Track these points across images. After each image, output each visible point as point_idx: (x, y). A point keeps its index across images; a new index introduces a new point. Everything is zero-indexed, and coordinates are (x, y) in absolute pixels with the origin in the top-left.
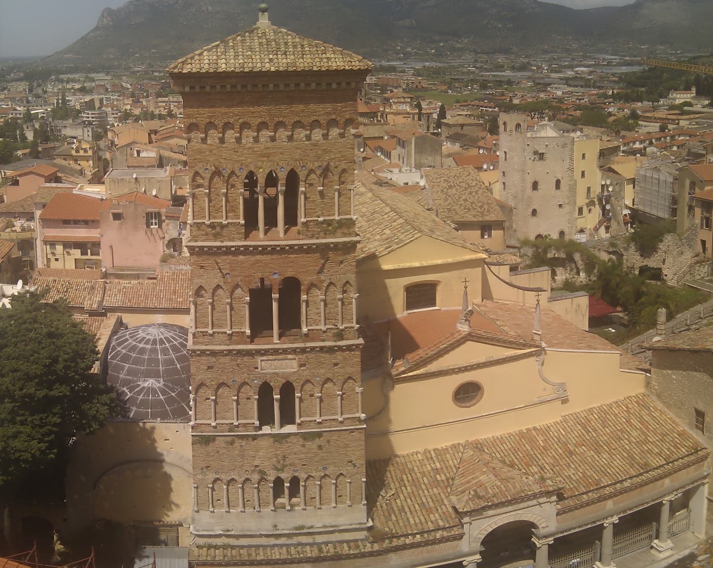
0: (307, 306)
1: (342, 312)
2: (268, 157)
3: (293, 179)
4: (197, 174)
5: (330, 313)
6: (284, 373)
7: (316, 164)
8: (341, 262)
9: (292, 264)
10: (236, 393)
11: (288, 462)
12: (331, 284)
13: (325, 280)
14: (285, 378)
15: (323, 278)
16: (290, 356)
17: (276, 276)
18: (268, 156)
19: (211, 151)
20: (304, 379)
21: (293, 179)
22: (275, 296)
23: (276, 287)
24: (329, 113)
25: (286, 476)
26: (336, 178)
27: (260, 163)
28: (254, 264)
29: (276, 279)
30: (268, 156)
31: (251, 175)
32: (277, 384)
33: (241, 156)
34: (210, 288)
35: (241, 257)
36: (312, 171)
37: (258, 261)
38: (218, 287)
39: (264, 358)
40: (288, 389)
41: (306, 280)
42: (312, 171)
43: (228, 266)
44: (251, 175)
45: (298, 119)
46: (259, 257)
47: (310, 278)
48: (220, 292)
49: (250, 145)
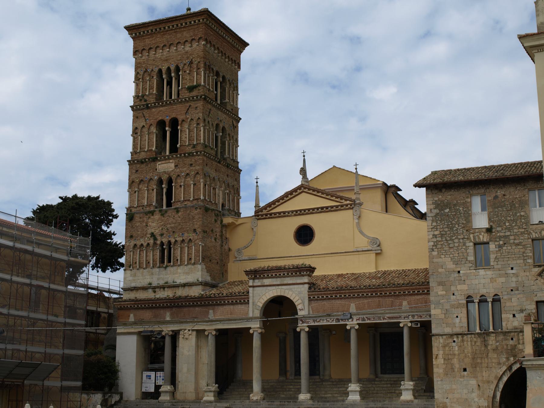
0: (181, 132)
1: (197, 136)
2: (167, 61)
3: (178, 69)
4: (138, 73)
5: (191, 136)
6: (168, 171)
7: (187, 61)
9: (175, 111)
10: (146, 186)
12: (192, 119)
13: (189, 118)
14: (168, 174)
15: (188, 116)
16: (171, 161)
17: (168, 118)
18: (167, 60)
19: (144, 62)
21: (178, 69)
22: (167, 128)
24: (192, 36)
25: (165, 240)
27: (163, 64)
28: (159, 112)
29: (167, 119)
30: (167, 60)
31: (160, 71)
32: (165, 178)
33: (156, 62)
34: (139, 128)
35: (154, 110)
36: (185, 64)
38: (144, 126)
39: (160, 163)
40: (170, 182)
41: (180, 118)
43: (148, 115)
44: (160, 71)
45: (179, 41)
46: (161, 108)
47: (182, 117)
49: (159, 57)
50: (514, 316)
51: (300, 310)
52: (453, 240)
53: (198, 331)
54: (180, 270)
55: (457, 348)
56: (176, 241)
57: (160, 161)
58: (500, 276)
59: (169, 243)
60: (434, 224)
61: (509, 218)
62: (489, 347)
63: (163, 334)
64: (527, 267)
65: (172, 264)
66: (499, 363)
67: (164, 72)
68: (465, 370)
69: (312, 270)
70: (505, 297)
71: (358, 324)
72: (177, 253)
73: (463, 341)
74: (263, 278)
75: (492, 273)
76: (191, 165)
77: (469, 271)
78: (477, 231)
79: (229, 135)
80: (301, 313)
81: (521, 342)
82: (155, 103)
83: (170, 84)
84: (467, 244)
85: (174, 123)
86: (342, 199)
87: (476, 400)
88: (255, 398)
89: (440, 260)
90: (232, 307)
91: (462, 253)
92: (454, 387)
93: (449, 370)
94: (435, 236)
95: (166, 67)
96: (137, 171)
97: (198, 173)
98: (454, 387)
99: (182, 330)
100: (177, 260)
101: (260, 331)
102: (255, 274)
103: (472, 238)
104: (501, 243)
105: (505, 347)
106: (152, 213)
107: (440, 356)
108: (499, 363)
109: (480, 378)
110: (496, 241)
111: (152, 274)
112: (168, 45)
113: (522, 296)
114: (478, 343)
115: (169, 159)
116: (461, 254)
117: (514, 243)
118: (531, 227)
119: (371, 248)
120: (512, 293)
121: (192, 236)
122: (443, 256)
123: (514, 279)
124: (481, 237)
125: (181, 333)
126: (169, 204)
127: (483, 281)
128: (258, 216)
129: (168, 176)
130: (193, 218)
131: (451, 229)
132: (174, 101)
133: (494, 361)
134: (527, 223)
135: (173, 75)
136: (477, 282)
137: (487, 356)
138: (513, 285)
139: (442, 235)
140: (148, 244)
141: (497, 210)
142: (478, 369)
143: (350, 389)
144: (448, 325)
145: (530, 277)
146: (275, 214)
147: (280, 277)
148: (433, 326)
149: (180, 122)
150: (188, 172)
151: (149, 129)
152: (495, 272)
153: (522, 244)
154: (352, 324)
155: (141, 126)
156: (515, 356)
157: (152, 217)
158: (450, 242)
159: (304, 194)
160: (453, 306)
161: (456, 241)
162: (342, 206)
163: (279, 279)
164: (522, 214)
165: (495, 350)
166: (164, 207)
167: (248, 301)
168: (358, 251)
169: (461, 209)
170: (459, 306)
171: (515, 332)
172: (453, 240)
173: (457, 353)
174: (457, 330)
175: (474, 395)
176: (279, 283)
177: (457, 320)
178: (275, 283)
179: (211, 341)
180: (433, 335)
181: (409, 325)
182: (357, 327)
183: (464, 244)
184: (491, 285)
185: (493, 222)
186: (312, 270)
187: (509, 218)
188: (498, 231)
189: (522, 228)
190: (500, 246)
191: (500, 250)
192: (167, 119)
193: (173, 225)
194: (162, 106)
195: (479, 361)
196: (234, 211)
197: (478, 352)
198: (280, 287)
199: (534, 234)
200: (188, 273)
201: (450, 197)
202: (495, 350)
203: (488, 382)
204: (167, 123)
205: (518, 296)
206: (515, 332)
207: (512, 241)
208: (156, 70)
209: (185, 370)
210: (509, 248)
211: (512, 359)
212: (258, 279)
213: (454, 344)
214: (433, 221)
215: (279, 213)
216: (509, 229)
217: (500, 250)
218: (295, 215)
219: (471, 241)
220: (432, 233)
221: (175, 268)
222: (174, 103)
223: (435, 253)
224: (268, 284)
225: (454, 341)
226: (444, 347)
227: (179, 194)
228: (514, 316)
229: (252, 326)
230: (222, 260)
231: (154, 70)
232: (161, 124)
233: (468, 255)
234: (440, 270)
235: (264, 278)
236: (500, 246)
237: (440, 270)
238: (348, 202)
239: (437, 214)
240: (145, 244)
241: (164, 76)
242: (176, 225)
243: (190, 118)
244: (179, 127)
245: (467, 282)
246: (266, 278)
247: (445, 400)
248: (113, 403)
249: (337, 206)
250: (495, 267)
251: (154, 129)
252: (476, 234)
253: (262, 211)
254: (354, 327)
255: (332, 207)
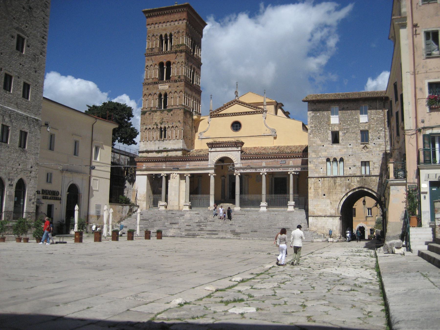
8: (181, 56)
11: (163, 121)
12: (179, 62)
16: (167, 84)
20: (170, 91)
21: (171, 35)
23: (165, 64)
26: (181, 34)
31: (161, 36)
32: (163, 93)
37: (161, 57)
38: (151, 65)
40: (166, 95)
41: (172, 62)
42: (175, 33)
44: (161, 36)
46: (162, 56)
48: (151, 66)
50: (350, 168)
51: (237, 164)
52: (320, 129)
53: (180, 174)
54: (171, 142)
55: (321, 184)
56: (169, 127)
57: (160, 84)
58: (344, 148)
59: (165, 128)
60: (312, 121)
61: (349, 119)
62: (337, 184)
63: (162, 175)
64: (357, 144)
65: (166, 139)
66: (342, 192)
67: (163, 36)
68: (324, 195)
69: (242, 144)
70: (346, 159)
71: (266, 172)
72: (169, 133)
73: (324, 181)
74: (216, 148)
75: (340, 146)
76: (178, 87)
77: (328, 146)
78: (333, 125)
79: (196, 72)
80: (236, 166)
81: (353, 181)
82: (158, 53)
83: (166, 43)
84: (328, 132)
85: (169, 64)
86: (257, 108)
87: (329, 210)
88: (211, 209)
89: (314, 139)
90: (199, 162)
91: (325, 136)
92: (319, 203)
93: (317, 194)
94: (312, 127)
95: (165, 34)
96: (148, 89)
97: (181, 91)
98: (319, 203)
99: (171, 173)
100: (169, 137)
101: (214, 175)
102: (212, 145)
103: (331, 129)
104: (345, 131)
105: (345, 184)
106: (156, 111)
107: (312, 188)
108: (342, 192)
109: (332, 199)
110: (342, 131)
111: (155, 144)
112: (166, 22)
113: (354, 158)
114: (332, 182)
115: (165, 83)
116: (325, 137)
117: (351, 132)
118: (360, 124)
119: (271, 134)
120: (350, 157)
121: (178, 124)
122: (315, 137)
123: (351, 150)
124: (335, 128)
125: (171, 175)
126: (165, 107)
127: (335, 151)
128: (212, 115)
129: (164, 92)
130: (179, 115)
131: (320, 123)
132: (169, 52)
133: (339, 190)
134: (358, 122)
135: (168, 38)
136: (332, 151)
137: (335, 189)
138: (350, 153)
139: (315, 127)
140: (153, 128)
141: (343, 115)
142: (331, 194)
143: (261, 205)
144: (317, 172)
145: (359, 149)
146: (221, 114)
147: (226, 147)
148: (309, 173)
149: (172, 64)
150: (176, 90)
151: (154, 66)
152: (341, 146)
153: (356, 132)
154: (264, 171)
155: (150, 65)
156: (349, 188)
157: (156, 114)
158: (319, 130)
159: (236, 104)
160: (319, 163)
161: (322, 130)
162: (257, 112)
163: (225, 148)
164: (356, 117)
165: (340, 185)
166: (163, 109)
167: (208, 159)
168: (265, 136)
169: (325, 114)
170: (322, 163)
171: (350, 177)
172: (320, 129)
173: (321, 186)
174: (321, 175)
175: (329, 207)
176: (225, 150)
177: (322, 170)
178: (222, 150)
179: (188, 179)
180: (309, 178)
181: (293, 173)
182: (266, 174)
183: (326, 132)
184: (339, 153)
185: (342, 121)
186: (242, 144)
187: (349, 119)
188: (344, 126)
189: (356, 125)
190: (345, 133)
191: (344, 135)
192: (165, 62)
193: (167, 118)
194: (162, 54)
195: (332, 190)
196: (197, 112)
197: (331, 186)
198: (225, 152)
199: (361, 128)
200: (175, 144)
201: (320, 107)
202: (340, 185)
203: (336, 201)
204: (165, 64)
205: (353, 159)
206: (350, 177)
207: (350, 131)
208: (159, 35)
209: (173, 194)
210: (349, 134)
211: (348, 190)
212: (214, 148)
213: (319, 182)
214: (311, 119)
215: (223, 114)
216: (350, 125)
217: (344, 135)
218: (231, 116)
219: (330, 130)
220: (310, 125)
221: (168, 141)
222: (170, 53)
223: (311, 136)
224: (219, 150)
225: (320, 181)
226: (314, 183)
227: (171, 102)
228: (350, 168)
229: (210, 172)
230: (192, 138)
231: (158, 35)
232: (161, 64)
233: (328, 138)
234: (314, 145)
235: (217, 147)
236: (345, 133)
237: (314, 145)
238: (260, 110)
239: (313, 116)
240: (151, 128)
241: (163, 39)
242: (169, 118)
243: (177, 62)
244: (171, 66)
245: (327, 151)
246: (218, 147)
247: (314, 210)
248: (134, 211)
249: (254, 112)
250: (342, 144)
251: (157, 67)
252: (333, 127)
253: (214, 113)
254: (264, 174)
255: (251, 112)
